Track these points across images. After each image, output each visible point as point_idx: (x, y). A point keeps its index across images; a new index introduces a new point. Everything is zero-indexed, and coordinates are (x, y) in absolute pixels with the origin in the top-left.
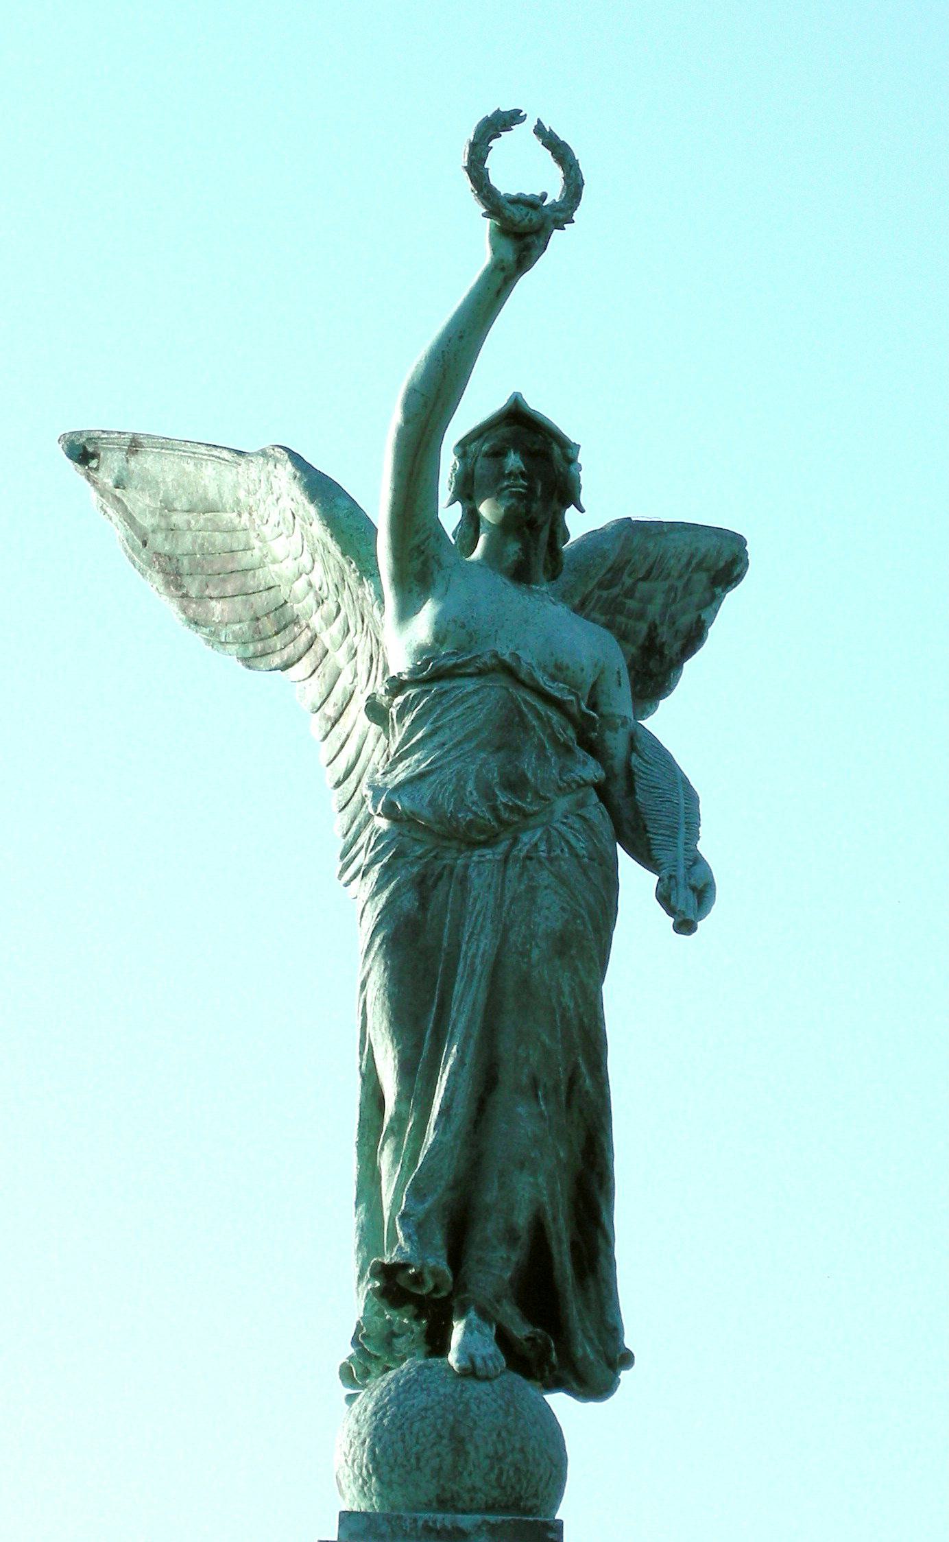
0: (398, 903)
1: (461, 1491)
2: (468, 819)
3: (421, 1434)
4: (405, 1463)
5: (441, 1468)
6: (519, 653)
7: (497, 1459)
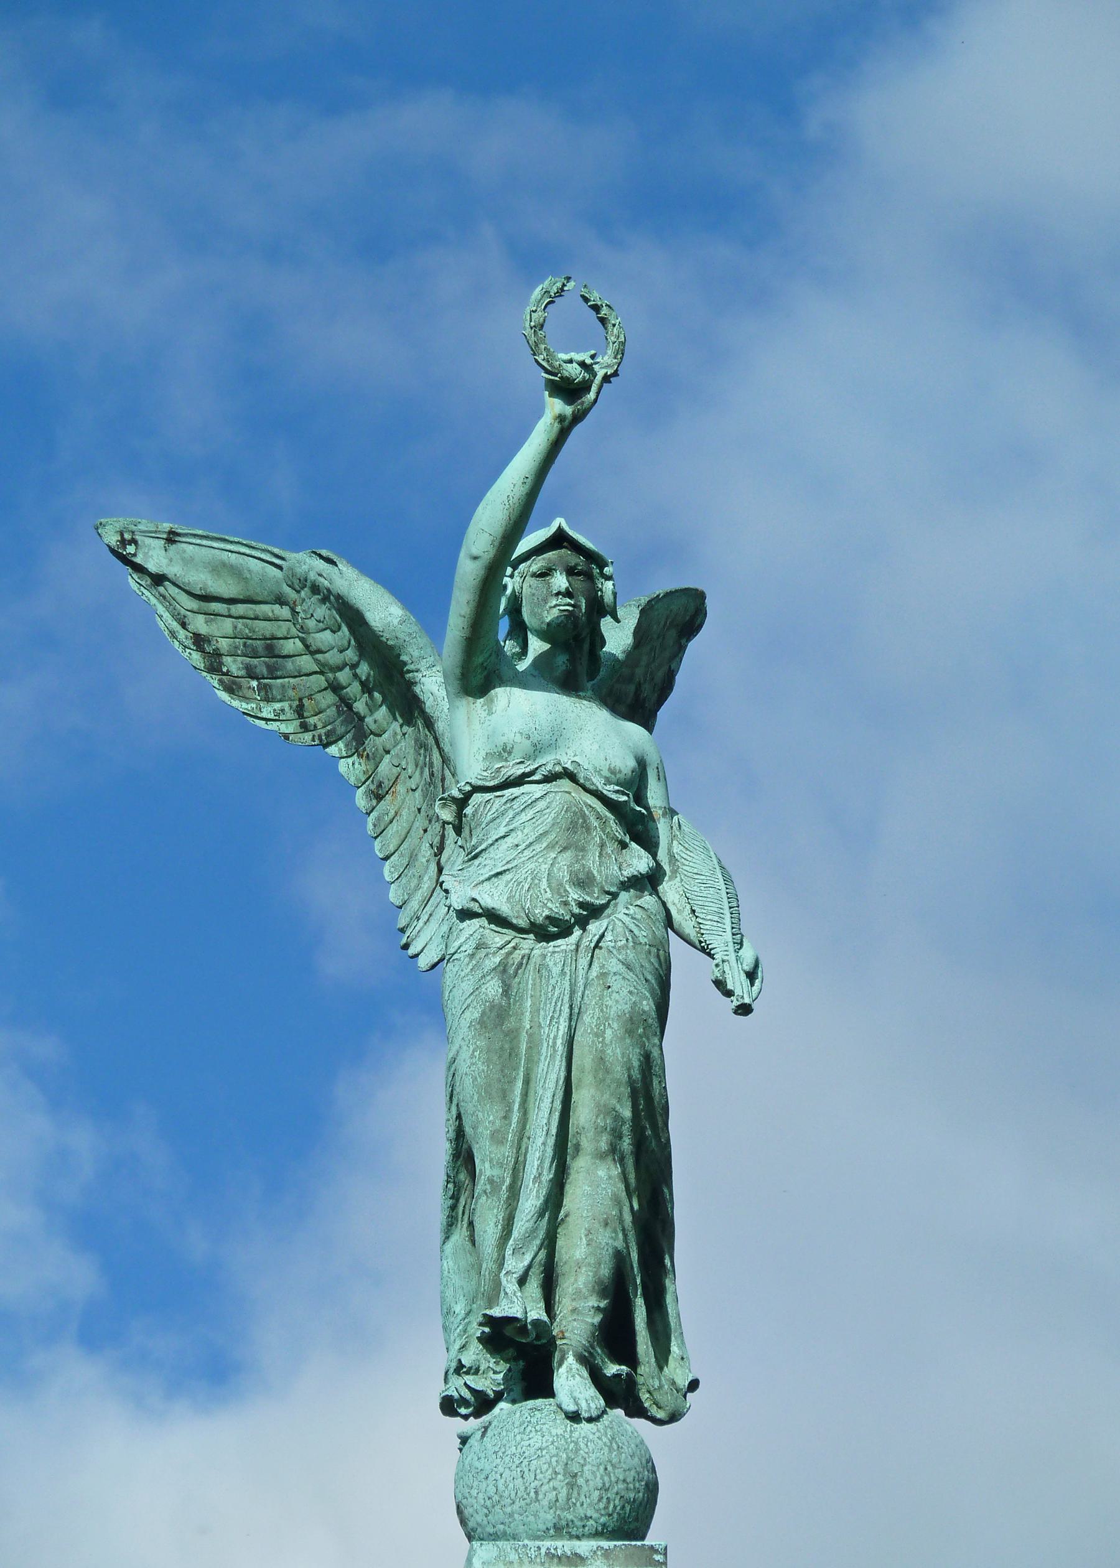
0: (483, 990)
1: (574, 1519)
2: (544, 915)
3: (538, 1471)
4: (525, 1496)
5: (557, 1500)
6: (576, 759)
7: (605, 1490)
